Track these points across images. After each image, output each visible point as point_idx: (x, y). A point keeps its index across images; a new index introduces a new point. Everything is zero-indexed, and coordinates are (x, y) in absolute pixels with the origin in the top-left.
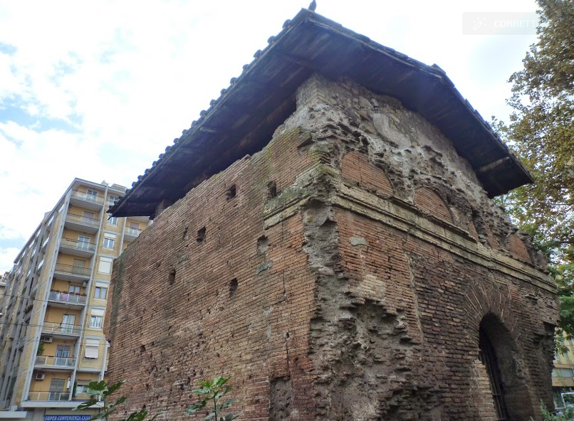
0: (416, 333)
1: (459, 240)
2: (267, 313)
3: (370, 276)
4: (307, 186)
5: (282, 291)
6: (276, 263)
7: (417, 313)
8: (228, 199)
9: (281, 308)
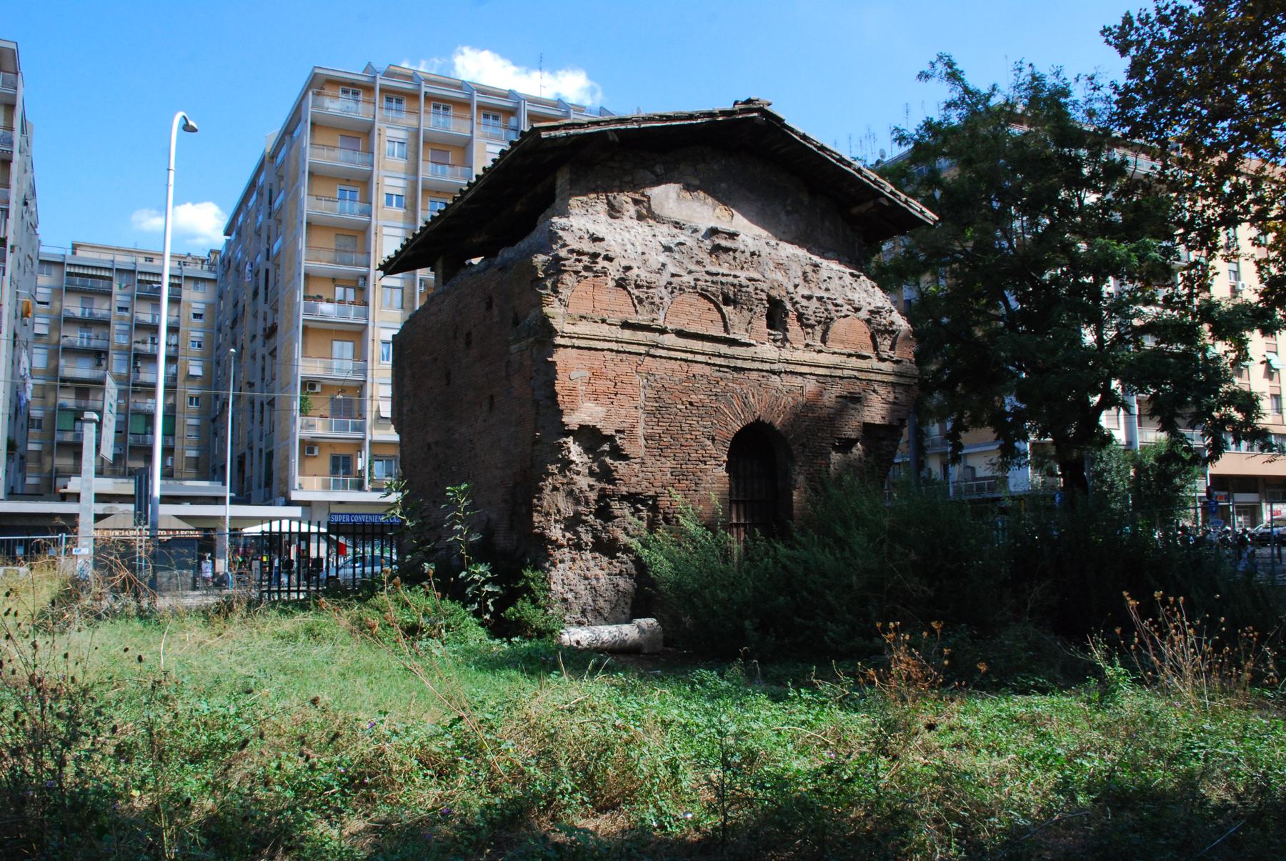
0: (637, 448)
1: (724, 349)
3: (590, 405)
7: (640, 431)
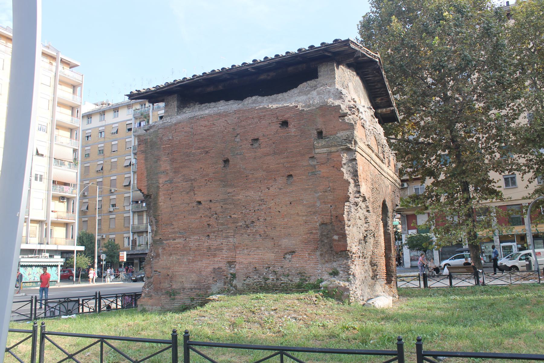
2: (317, 195)
4: (345, 139)
5: (328, 186)
6: (323, 172)
8: (280, 127)
9: (326, 194)
